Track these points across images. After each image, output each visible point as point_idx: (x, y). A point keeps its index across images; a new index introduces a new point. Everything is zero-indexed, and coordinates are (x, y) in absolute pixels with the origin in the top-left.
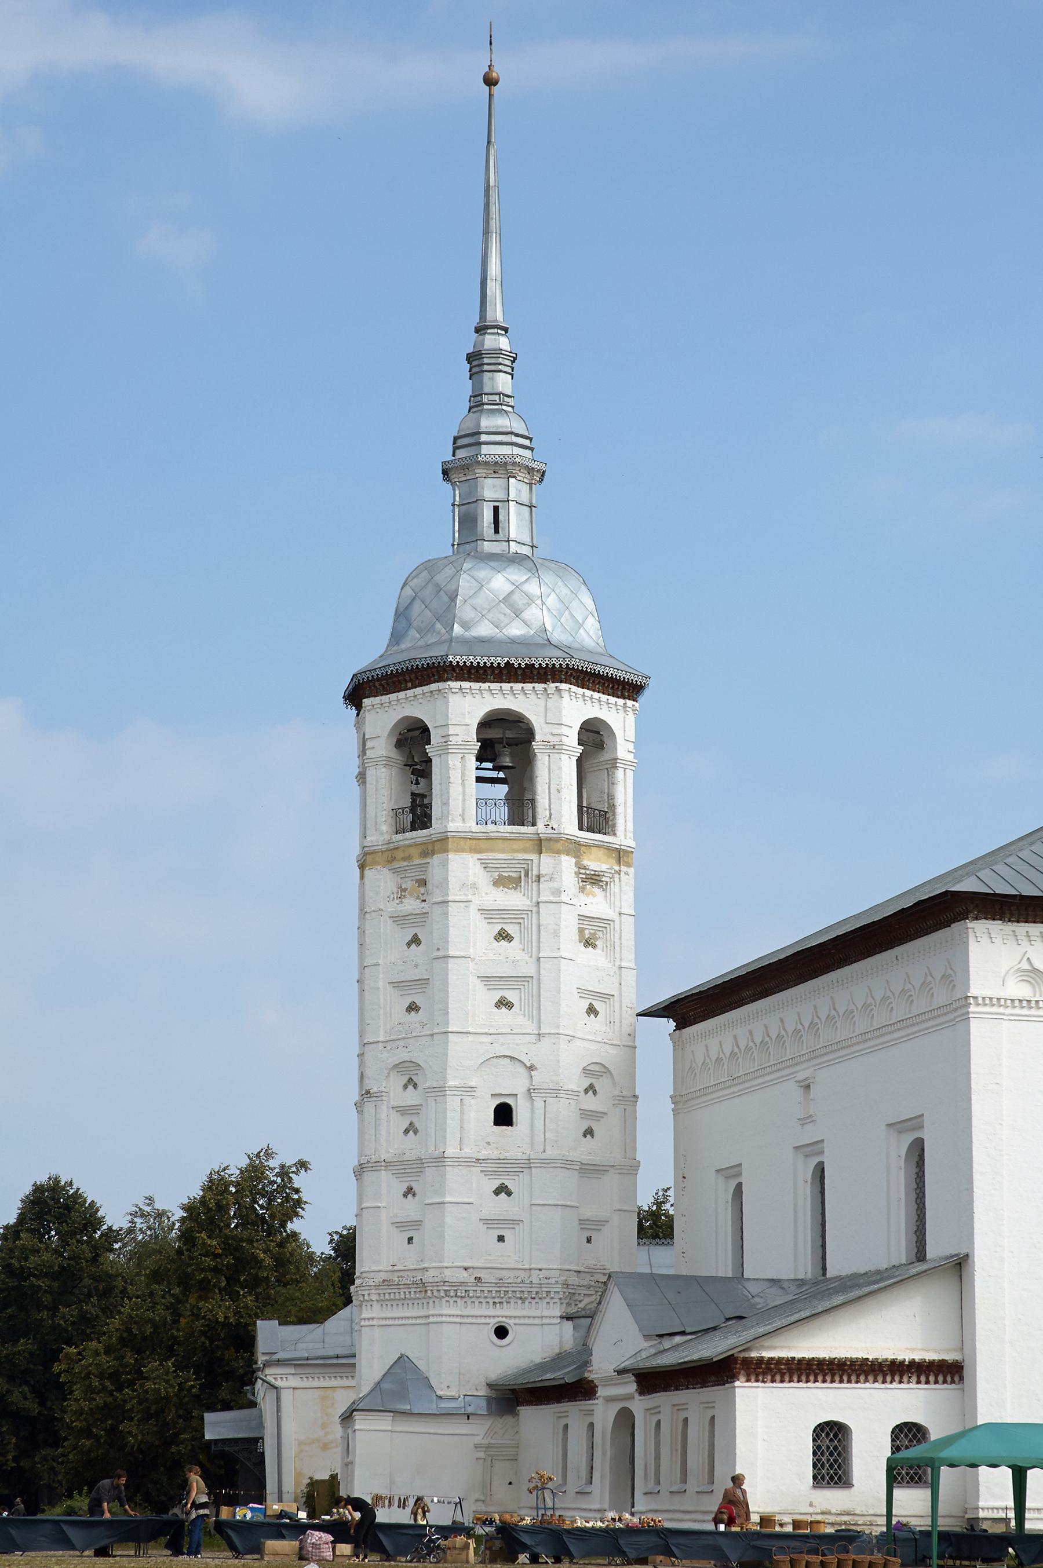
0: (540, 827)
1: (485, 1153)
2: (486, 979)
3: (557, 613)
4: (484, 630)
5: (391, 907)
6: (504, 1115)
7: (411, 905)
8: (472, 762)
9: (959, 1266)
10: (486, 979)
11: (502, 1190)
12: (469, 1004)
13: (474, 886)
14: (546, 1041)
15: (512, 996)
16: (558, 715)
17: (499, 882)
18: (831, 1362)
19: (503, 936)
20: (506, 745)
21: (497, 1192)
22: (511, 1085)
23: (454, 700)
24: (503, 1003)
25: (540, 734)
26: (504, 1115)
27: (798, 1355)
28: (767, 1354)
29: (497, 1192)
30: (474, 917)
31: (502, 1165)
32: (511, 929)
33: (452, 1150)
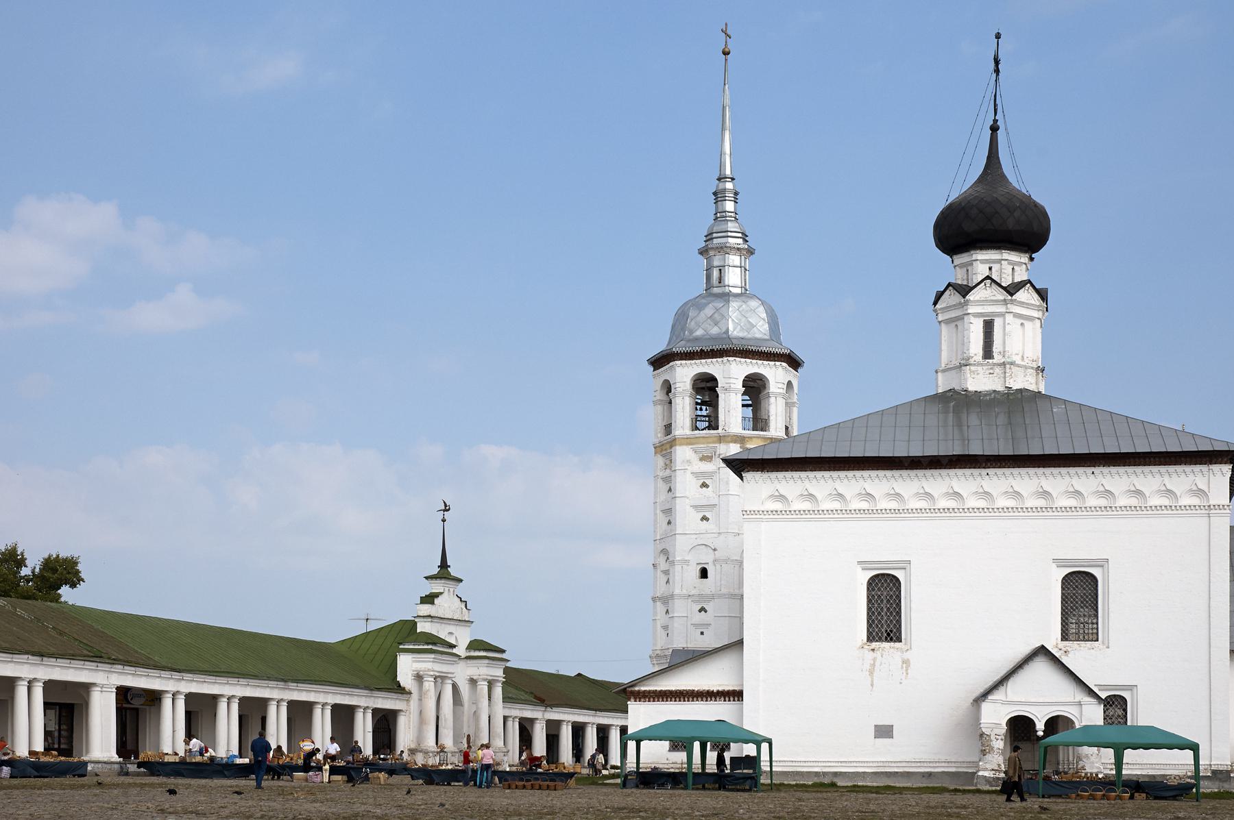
0: (720, 430)
1: (693, 592)
2: (695, 507)
3: (745, 321)
4: (699, 333)
5: (661, 474)
6: (704, 573)
7: (668, 472)
8: (740, 397)
9: (740, 643)
10: (695, 507)
11: (702, 610)
12: (687, 519)
13: (689, 462)
14: (722, 536)
15: (708, 515)
16: (731, 374)
17: (701, 459)
18: (676, 691)
19: (704, 485)
20: (706, 388)
21: (700, 611)
22: (706, 558)
23: (679, 370)
24: (705, 518)
25: (721, 383)
26: (704, 573)
27: (659, 689)
28: (643, 689)
29: (700, 611)
30: (688, 475)
31: (701, 597)
32: (708, 482)
33: (677, 591)
